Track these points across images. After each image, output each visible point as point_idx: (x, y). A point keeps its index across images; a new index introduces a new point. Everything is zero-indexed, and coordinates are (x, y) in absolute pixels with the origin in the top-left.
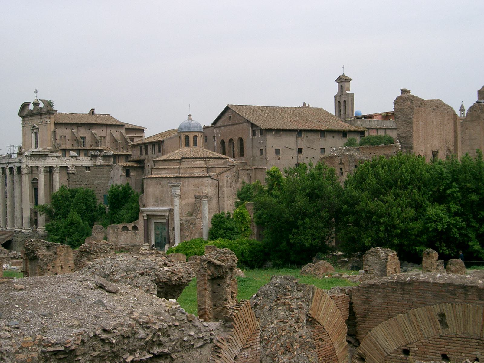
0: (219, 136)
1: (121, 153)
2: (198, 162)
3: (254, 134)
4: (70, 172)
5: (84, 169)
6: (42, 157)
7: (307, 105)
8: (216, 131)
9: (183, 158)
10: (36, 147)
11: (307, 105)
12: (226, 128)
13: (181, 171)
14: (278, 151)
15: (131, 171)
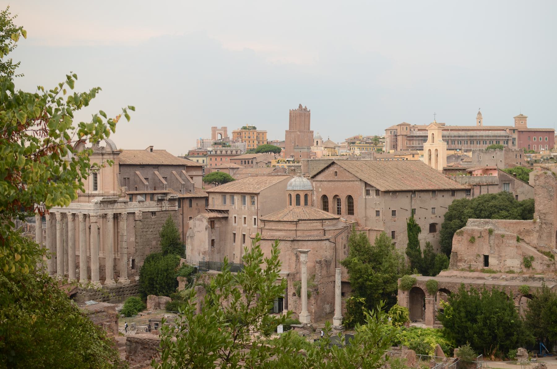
0: (320, 190)
1: (185, 196)
2: (315, 224)
3: (368, 193)
4: (137, 218)
5: (150, 215)
6: (111, 203)
7: (304, 107)
8: (316, 185)
9: (299, 220)
10: (96, 188)
11: (304, 107)
12: (330, 183)
13: (299, 233)
14: (394, 213)
15: (215, 222)
